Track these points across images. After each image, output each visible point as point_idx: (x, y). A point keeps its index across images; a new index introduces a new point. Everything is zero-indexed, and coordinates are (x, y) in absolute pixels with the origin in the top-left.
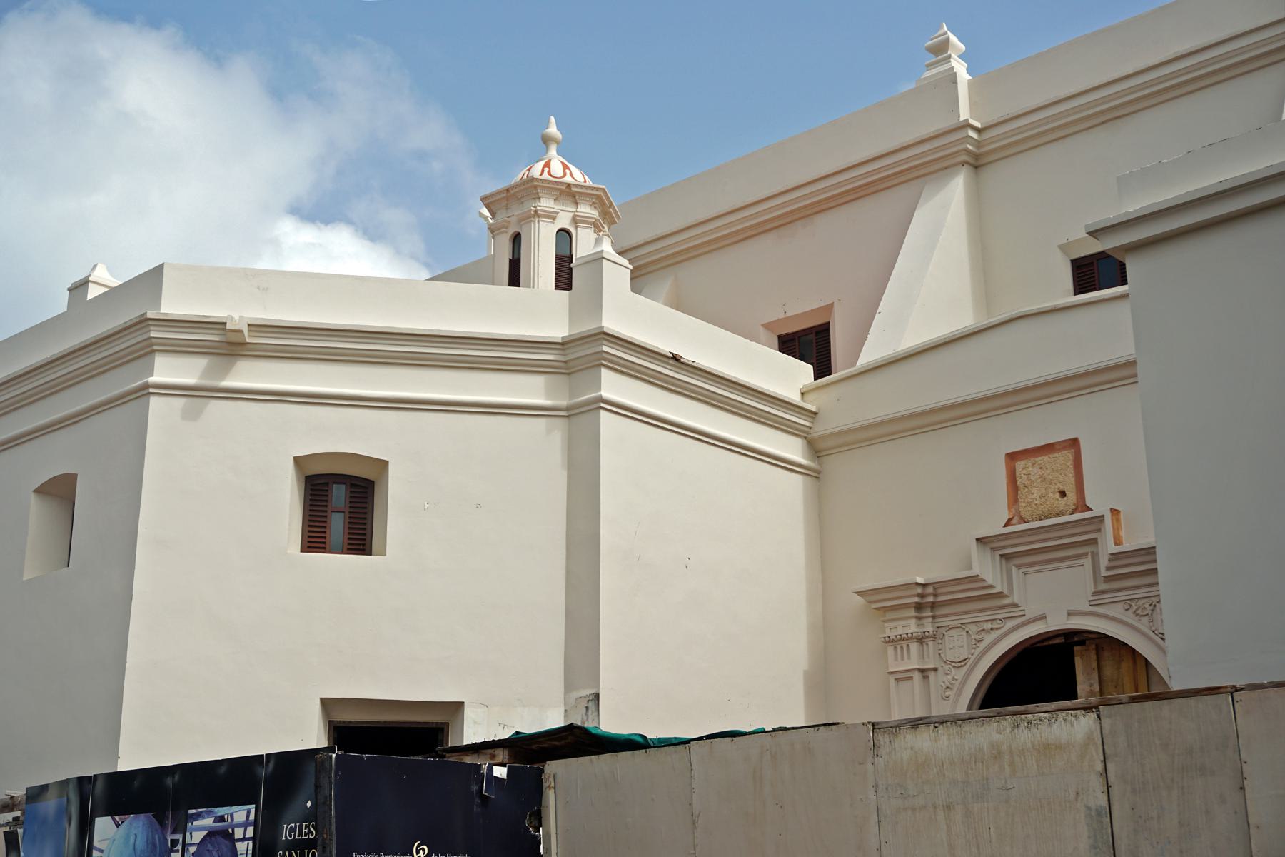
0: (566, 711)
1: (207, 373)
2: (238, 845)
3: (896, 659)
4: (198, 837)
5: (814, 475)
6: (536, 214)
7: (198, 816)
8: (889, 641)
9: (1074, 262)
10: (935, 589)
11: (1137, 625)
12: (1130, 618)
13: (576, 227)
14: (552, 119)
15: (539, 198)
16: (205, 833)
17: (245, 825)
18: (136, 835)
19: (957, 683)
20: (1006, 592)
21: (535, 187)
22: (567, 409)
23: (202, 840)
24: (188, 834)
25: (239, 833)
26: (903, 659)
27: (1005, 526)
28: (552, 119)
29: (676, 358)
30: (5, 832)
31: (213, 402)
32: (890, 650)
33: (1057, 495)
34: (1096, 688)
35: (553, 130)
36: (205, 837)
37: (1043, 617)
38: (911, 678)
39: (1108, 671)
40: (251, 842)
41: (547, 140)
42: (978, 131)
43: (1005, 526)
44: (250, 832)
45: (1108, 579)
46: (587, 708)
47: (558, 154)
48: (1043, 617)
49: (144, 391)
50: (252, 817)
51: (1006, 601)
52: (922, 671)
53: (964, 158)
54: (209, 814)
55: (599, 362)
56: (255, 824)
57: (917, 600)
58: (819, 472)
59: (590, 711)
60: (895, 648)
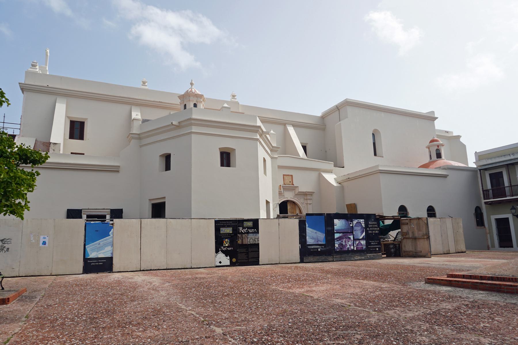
4: (355, 223)
7: (355, 220)
12: (297, 200)
17: (363, 222)
25: (362, 223)
37: (287, 198)
44: (364, 223)
45: (296, 194)
48: (287, 198)
50: (364, 221)
51: (282, 195)
54: (356, 220)
56: (365, 222)
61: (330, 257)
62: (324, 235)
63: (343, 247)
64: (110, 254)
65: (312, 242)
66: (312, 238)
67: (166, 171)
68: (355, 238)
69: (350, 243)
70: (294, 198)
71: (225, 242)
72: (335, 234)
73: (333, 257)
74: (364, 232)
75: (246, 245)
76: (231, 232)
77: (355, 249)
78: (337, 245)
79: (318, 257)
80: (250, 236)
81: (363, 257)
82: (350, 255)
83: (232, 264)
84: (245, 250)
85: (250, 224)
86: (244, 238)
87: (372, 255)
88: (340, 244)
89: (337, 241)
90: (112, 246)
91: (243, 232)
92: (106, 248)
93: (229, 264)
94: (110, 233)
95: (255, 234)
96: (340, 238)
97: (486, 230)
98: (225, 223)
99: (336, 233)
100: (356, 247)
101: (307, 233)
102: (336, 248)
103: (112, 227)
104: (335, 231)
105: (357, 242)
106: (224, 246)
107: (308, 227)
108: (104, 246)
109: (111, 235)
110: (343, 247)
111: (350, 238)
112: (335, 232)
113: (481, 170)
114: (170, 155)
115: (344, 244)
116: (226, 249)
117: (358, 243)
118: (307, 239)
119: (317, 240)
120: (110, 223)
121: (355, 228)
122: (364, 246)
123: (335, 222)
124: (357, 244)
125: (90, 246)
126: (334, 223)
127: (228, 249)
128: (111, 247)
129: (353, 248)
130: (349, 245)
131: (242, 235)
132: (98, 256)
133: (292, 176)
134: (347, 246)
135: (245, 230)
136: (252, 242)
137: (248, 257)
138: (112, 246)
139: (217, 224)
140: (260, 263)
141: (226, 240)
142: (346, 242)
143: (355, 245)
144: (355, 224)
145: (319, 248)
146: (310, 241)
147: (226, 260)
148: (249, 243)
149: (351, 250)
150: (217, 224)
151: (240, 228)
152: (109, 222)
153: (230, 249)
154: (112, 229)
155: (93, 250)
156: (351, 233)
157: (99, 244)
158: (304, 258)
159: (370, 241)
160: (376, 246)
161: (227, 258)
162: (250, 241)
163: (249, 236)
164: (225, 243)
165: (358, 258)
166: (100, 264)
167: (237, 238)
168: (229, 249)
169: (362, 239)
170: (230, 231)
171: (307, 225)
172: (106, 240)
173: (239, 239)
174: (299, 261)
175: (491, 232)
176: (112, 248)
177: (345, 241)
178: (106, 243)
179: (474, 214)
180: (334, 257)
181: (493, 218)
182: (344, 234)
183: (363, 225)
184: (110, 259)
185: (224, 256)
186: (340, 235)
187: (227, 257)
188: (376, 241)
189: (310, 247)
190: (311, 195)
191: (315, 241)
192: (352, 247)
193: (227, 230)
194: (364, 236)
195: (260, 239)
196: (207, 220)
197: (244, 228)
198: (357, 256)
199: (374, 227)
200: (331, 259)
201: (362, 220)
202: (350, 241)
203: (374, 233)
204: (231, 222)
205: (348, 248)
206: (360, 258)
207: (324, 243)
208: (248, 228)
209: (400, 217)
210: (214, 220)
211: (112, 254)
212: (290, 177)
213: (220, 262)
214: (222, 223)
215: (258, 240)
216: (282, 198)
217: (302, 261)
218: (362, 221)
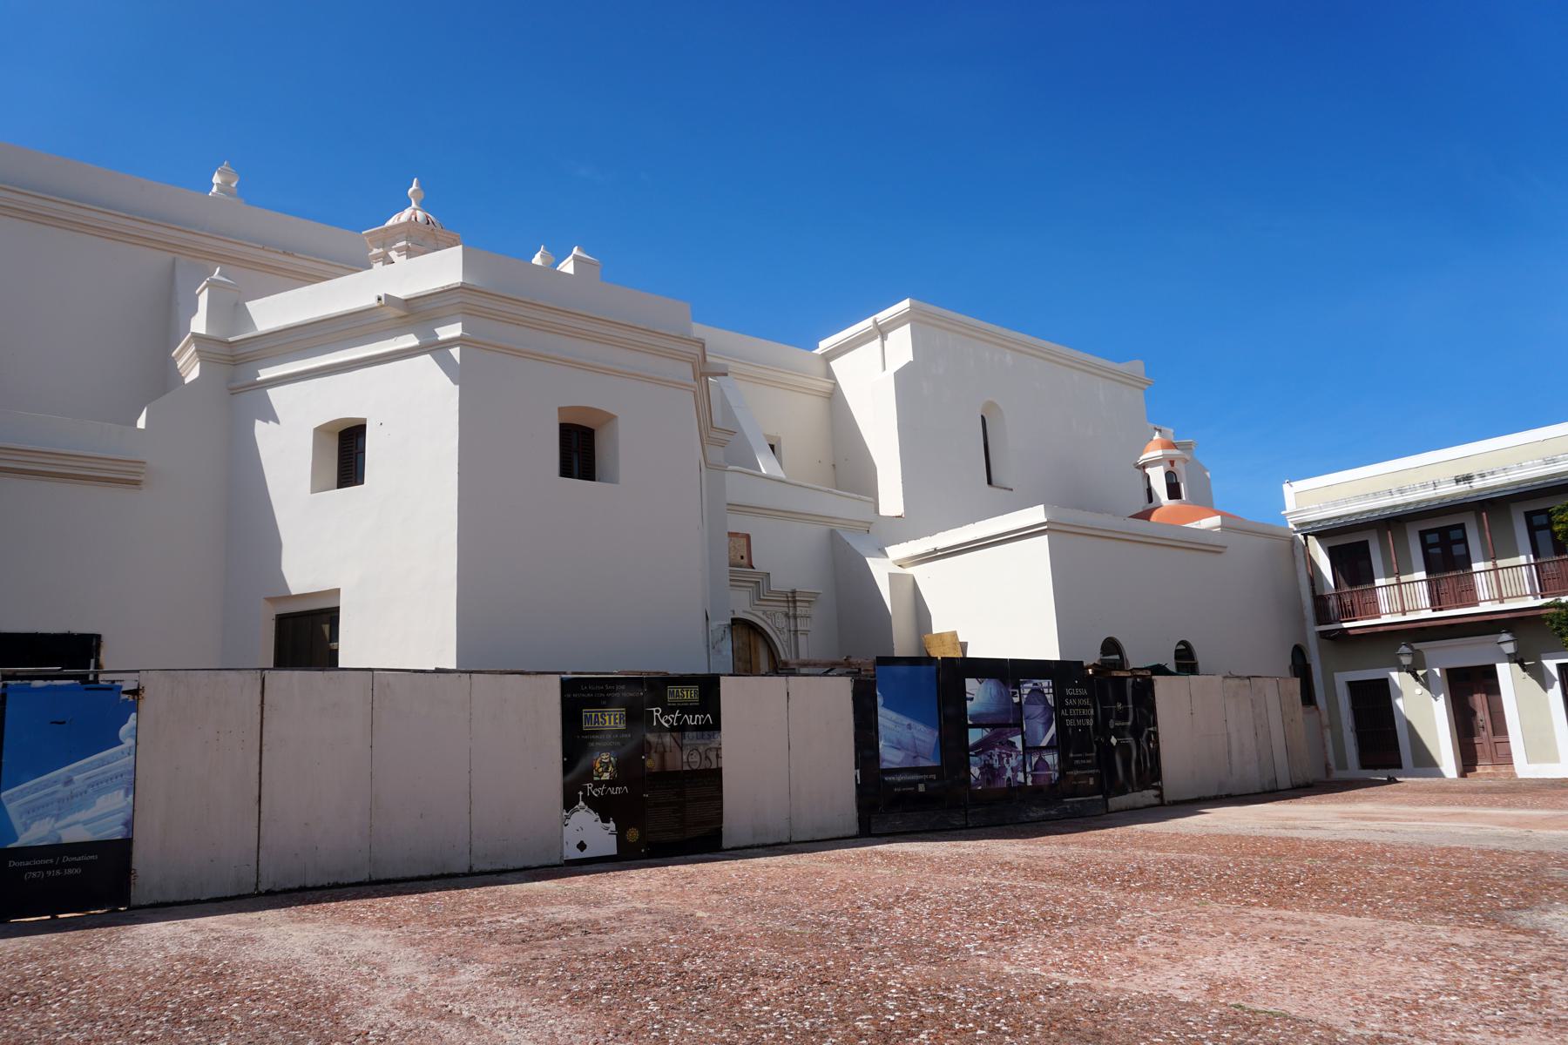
4: (1027, 691)
7: (1025, 682)
12: (764, 617)
17: (1048, 687)
23: (1030, 692)
25: (1046, 691)
34: (741, 645)
44: (1051, 691)
50: (1051, 685)
54: (1030, 682)
56: (1053, 687)
62: (937, 734)
64: (121, 827)
65: (897, 760)
66: (898, 746)
67: (338, 488)
68: (1028, 745)
69: (1013, 762)
71: (598, 765)
72: (971, 731)
73: (966, 814)
74: (1052, 723)
77: (1029, 783)
78: (975, 771)
85: (690, 694)
87: (1078, 802)
89: (976, 755)
90: (132, 788)
91: (666, 725)
92: (103, 798)
93: (614, 852)
94: (123, 731)
95: (706, 733)
96: (984, 745)
97: (1320, 715)
98: (601, 691)
99: (973, 727)
103: (134, 707)
106: (596, 779)
108: (90, 790)
109: (129, 742)
110: (994, 776)
111: (1013, 744)
112: (970, 722)
113: (1309, 537)
114: (364, 426)
115: (996, 765)
116: (605, 791)
117: (1037, 762)
118: (880, 751)
119: (914, 754)
120: (124, 689)
122: (1054, 770)
123: (967, 690)
124: (1033, 764)
125: (21, 791)
127: (612, 793)
128: (127, 795)
129: (1023, 781)
130: (1015, 770)
132: (60, 838)
133: (748, 537)
134: (1005, 773)
135: (673, 719)
136: (695, 762)
140: (726, 844)
142: (1003, 758)
143: (1028, 769)
144: (1028, 694)
146: (890, 756)
147: (598, 834)
148: (686, 768)
149: (1016, 785)
151: (654, 709)
152: (117, 683)
154: (133, 715)
155: (35, 812)
156: (1015, 725)
157: (69, 782)
158: (873, 821)
161: (607, 829)
162: (690, 760)
163: (685, 742)
164: (600, 770)
166: (70, 871)
170: (617, 721)
171: (880, 700)
172: (103, 762)
173: (653, 751)
174: (854, 830)
175: (1335, 725)
176: (131, 796)
177: (1001, 759)
178: (101, 777)
179: (1290, 668)
180: (969, 812)
181: (1342, 678)
186: (986, 733)
187: (608, 822)
189: (890, 778)
190: (807, 604)
195: (724, 753)
196: (533, 678)
197: (668, 710)
198: (1036, 806)
201: (1045, 683)
203: (1082, 727)
205: (1009, 778)
207: (936, 765)
208: (687, 709)
209: (1149, 673)
210: (556, 680)
211: (129, 824)
212: (743, 541)
213: (582, 846)
214: (590, 691)
215: (718, 757)
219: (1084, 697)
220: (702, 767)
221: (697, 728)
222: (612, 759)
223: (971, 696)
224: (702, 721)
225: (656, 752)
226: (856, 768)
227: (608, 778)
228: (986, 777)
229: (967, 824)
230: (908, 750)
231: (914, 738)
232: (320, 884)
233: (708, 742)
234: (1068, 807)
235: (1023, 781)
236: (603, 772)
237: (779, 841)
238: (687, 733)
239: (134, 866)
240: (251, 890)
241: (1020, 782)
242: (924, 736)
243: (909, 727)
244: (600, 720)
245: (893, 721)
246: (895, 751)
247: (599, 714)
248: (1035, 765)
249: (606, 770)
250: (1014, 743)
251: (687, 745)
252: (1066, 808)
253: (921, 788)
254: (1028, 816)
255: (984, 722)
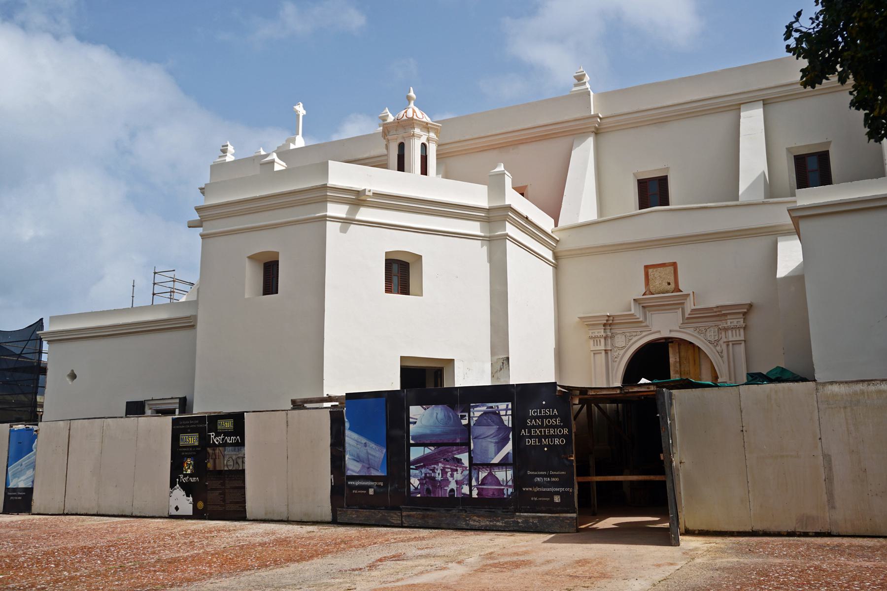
0: (492, 364)
1: (348, 213)
2: (503, 417)
3: (594, 345)
4: (478, 414)
5: (556, 267)
6: (413, 135)
7: (477, 406)
8: (591, 338)
9: (638, 180)
10: (613, 318)
11: (699, 337)
12: (695, 334)
13: (429, 143)
14: (411, 88)
15: (414, 128)
16: (482, 413)
17: (507, 410)
18: (437, 414)
19: (620, 356)
20: (643, 321)
21: (413, 123)
22: (489, 237)
24: (472, 414)
25: (503, 413)
26: (597, 345)
27: (643, 295)
28: (411, 88)
29: (527, 218)
30: (330, 411)
31: (352, 225)
32: (591, 342)
33: (667, 284)
34: (678, 360)
35: (412, 94)
36: (482, 414)
37: (659, 332)
38: (601, 353)
39: (682, 354)
40: (510, 417)
41: (409, 99)
42: (600, 119)
43: (643, 295)
44: (510, 412)
45: (688, 318)
46: (503, 363)
47: (415, 105)
48: (659, 332)
49: (324, 219)
50: (510, 406)
51: (644, 324)
52: (605, 350)
53: (593, 130)
54: (483, 406)
55: (505, 218)
56: (512, 409)
57: (605, 322)
58: (556, 265)
59: (504, 365)
60: (594, 341)
61: (395, 514)
62: (385, 451)
63: (434, 486)
66: (358, 459)
69: (458, 476)
70: (682, 330)
71: (186, 465)
73: (402, 516)
75: (220, 472)
76: (197, 444)
78: (415, 482)
79: (366, 512)
80: (229, 451)
81: (498, 521)
82: (454, 511)
83: (198, 515)
84: (220, 484)
85: (228, 425)
86: (217, 457)
87: (533, 517)
88: (426, 477)
90: (34, 469)
91: (217, 443)
93: (191, 513)
95: (237, 448)
96: (425, 461)
99: (416, 445)
100: (478, 489)
101: (347, 445)
102: (412, 488)
104: (412, 439)
105: (482, 475)
106: (184, 472)
107: (349, 429)
109: (35, 450)
110: (434, 486)
111: (459, 461)
112: (411, 442)
117: (485, 478)
118: (347, 462)
119: (367, 466)
121: (477, 431)
122: (507, 485)
123: (411, 416)
124: (480, 479)
126: (408, 417)
129: (468, 493)
131: (214, 450)
133: (674, 265)
135: (220, 439)
137: (224, 501)
138: (34, 469)
139: (175, 427)
141: (189, 461)
142: (447, 472)
143: (474, 483)
145: (371, 487)
146: (353, 467)
148: (226, 469)
150: (175, 427)
151: (211, 434)
153: (193, 480)
154: (36, 440)
156: (461, 444)
159: (529, 473)
160: (552, 489)
161: (188, 500)
162: (228, 464)
163: (226, 453)
164: (187, 468)
165: (482, 524)
167: (206, 456)
168: (193, 480)
169: (503, 464)
171: (347, 425)
173: (210, 458)
177: (444, 472)
182: (441, 448)
183: (507, 421)
184: (29, 491)
185: (184, 495)
186: (428, 451)
187: (189, 497)
188: (552, 473)
189: (351, 483)
191: (363, 465)
192: (466, 490)
193: (190, 439)
194: (508, 453)
198: (478, 516)
199: (547, 426)
200: (396, 519)
201: (502, 406)
202: (460, 470)
203: (548, 446)
204: (197, 422)
205: (452, 490)
206: (488, 523)
207: (383, 475)
208: (227, 434)
212: (671, 269)
215: (243, 462)
216: (644, 334)
217: (335, 522)
218: (504, 408)
219: (555, 417)
220: (234, 469)
221: (232, 445)
222: (192, 462)
223: (415, 420)
224: (235, 440)
225: (212, 459)
226: (331, 474)
227: (190, 473)
228: (426, 486)
229: (402, 523)
230: (363, 462)
231: (368, 453)
232: (81, 513)
233: (238, 453)
234: (520, 521)
235: (468, 493)
236: (188, 469)
237: (281, 519)
238: (227, 448)
239: (33, 498)
240: (62, 513)
241: (464, 494)
242: (378, 453)
243: (365, 445)
244: (187, 440)
245: (355, 440)
246: (355, 463)
247: (187, 437)
248: (483, 480)
249: (189, 468)
250: (461, 460)
251: (227, 455)
252: (518, 523)
253: (371, 492)
254: (468, 525)
255: (428, 442)
